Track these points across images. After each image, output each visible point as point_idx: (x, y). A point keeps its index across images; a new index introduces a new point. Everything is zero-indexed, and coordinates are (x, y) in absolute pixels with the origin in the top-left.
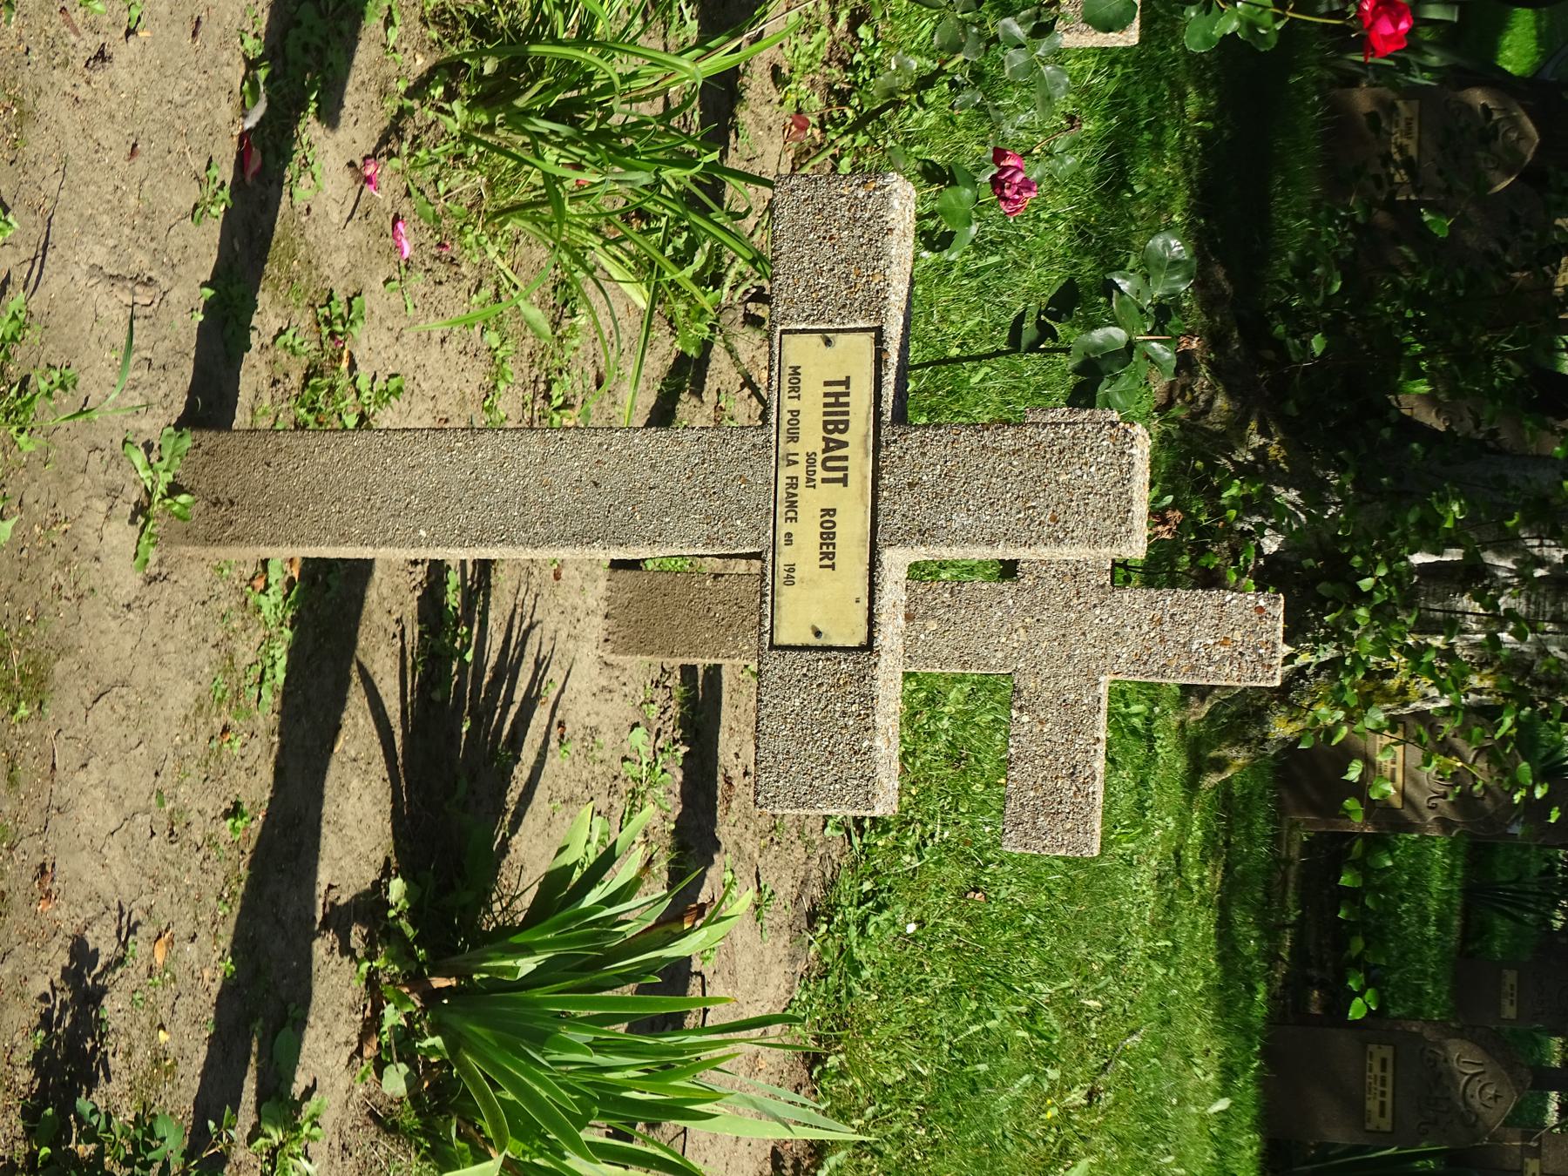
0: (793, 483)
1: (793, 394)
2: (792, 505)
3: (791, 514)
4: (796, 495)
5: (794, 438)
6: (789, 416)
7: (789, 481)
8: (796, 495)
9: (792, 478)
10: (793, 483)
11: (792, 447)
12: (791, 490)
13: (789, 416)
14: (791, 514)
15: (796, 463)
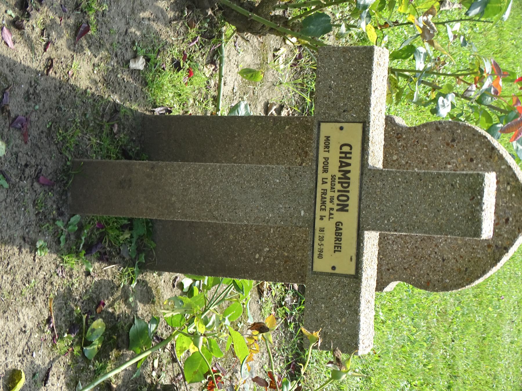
0: (325, 192)
1: (326, 150)
2: (323, 203)
3: (323, 207)
4: (326, 198)
5: (325, 171)
6: (324, 160)
7: (323, 191)
8: (326, 198)
9: (324, 190)
10: (325, 192)
11: (325, 175)
12: (323, 196)
13: (324, 160)
14: (323, 207)
15: (326, 183)
